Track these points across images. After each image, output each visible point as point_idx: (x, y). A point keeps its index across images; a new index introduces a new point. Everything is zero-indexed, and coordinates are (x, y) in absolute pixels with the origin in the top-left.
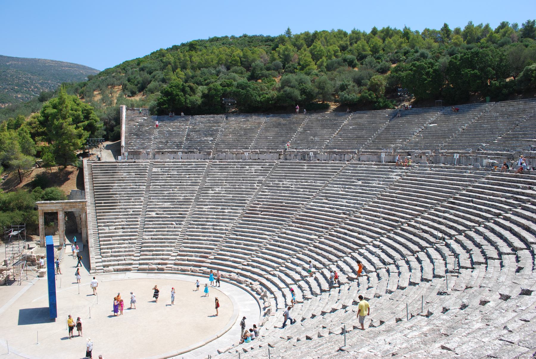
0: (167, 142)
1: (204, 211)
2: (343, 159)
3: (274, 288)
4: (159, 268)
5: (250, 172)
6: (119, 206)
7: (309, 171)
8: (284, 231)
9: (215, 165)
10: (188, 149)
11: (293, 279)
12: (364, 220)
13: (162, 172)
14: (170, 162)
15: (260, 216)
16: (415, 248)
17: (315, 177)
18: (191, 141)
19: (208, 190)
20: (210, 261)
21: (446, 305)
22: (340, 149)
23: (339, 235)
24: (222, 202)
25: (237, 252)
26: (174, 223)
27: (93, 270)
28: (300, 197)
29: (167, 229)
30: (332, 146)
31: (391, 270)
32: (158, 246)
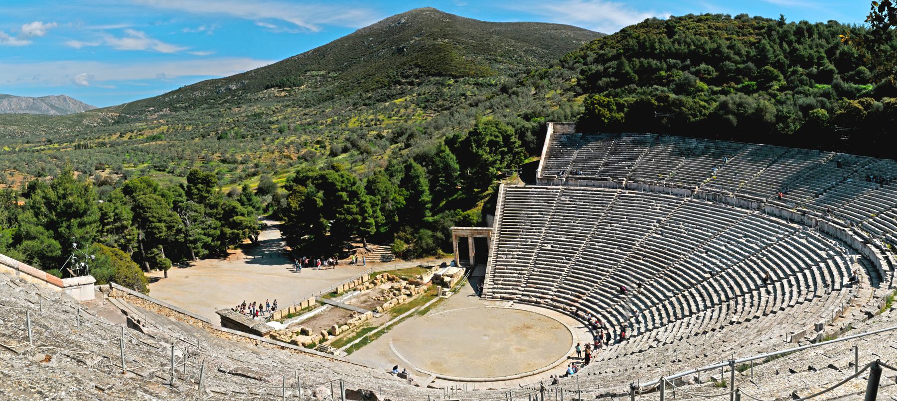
1: (596, 249)
6: (521, 235)
9: (623, 196)
24: (615, 241)
26: (564, 258)
29: (555, 264)
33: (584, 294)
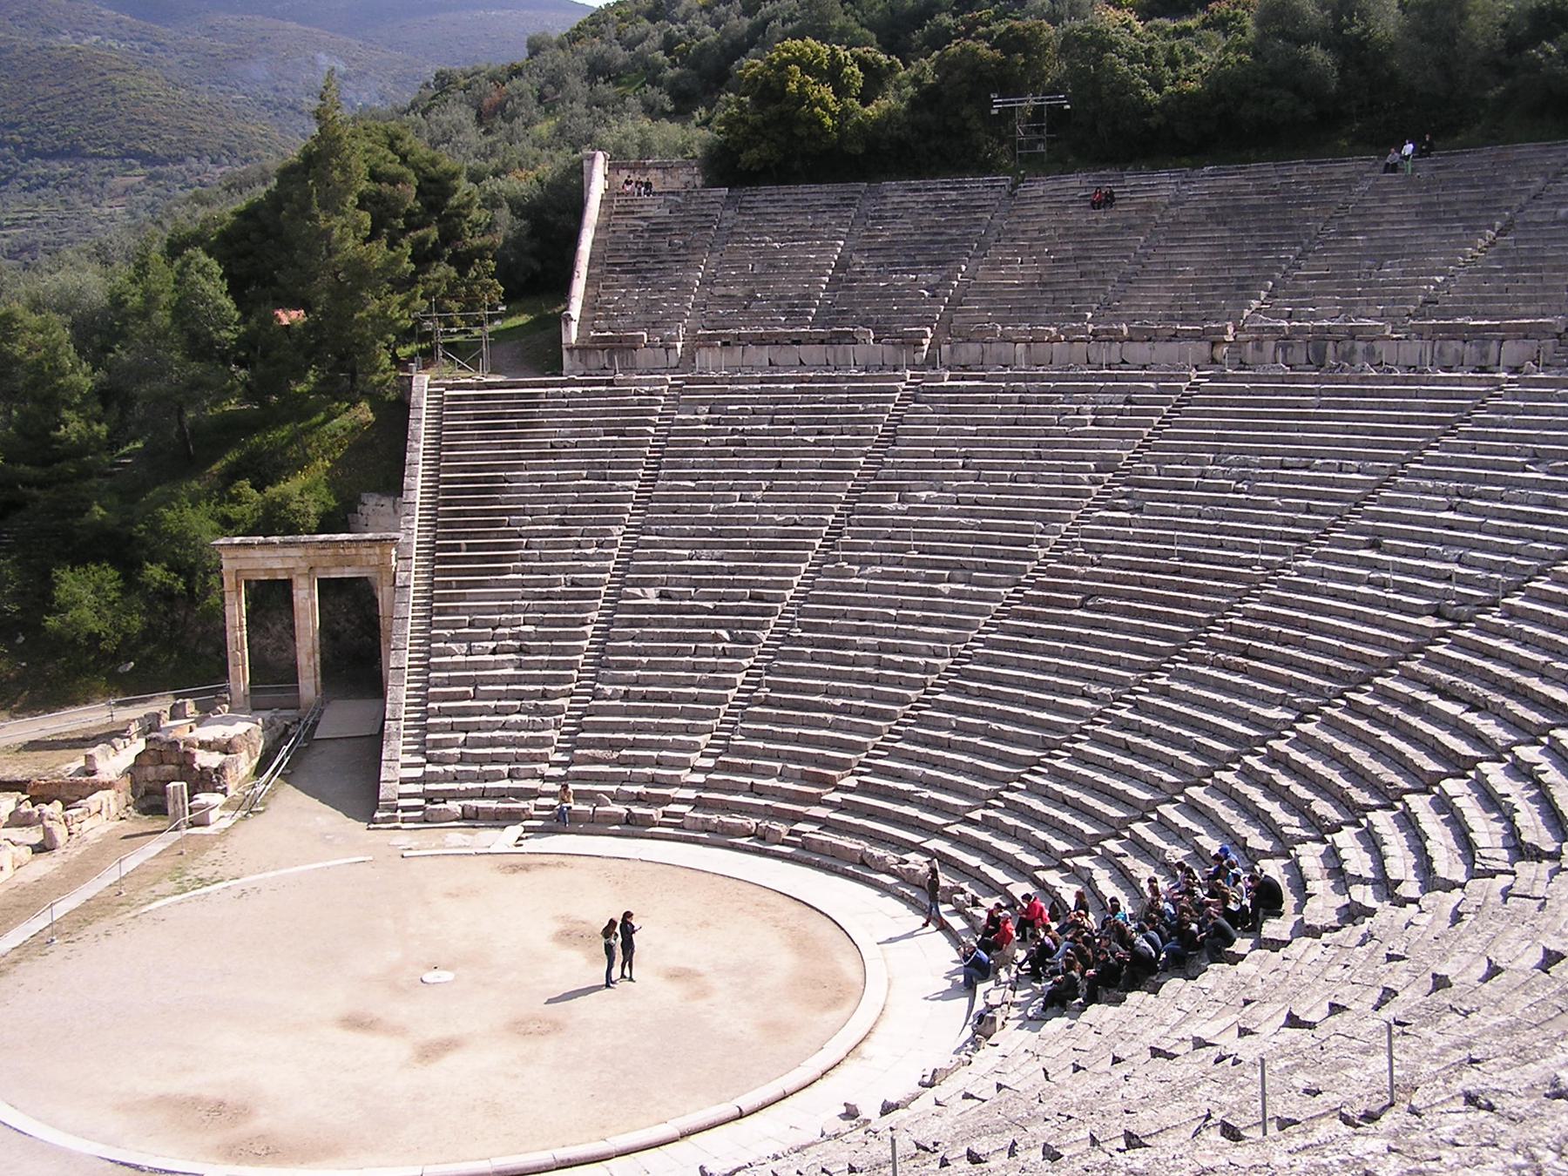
0: (751, 297)
2: (1492, 359)
5: (1074, 423)
7: (1328, 417)
9: (932, 390)
10: (834, 323)
14: (752, 381)
17: (1348, 443)
18: (851, 288)
20: (836, 797)
22: (1485, 316)
25: (954, 767)
27: (387, 808)
28: (1263, 535)
30: (1455, 300)
33: (842, 765)
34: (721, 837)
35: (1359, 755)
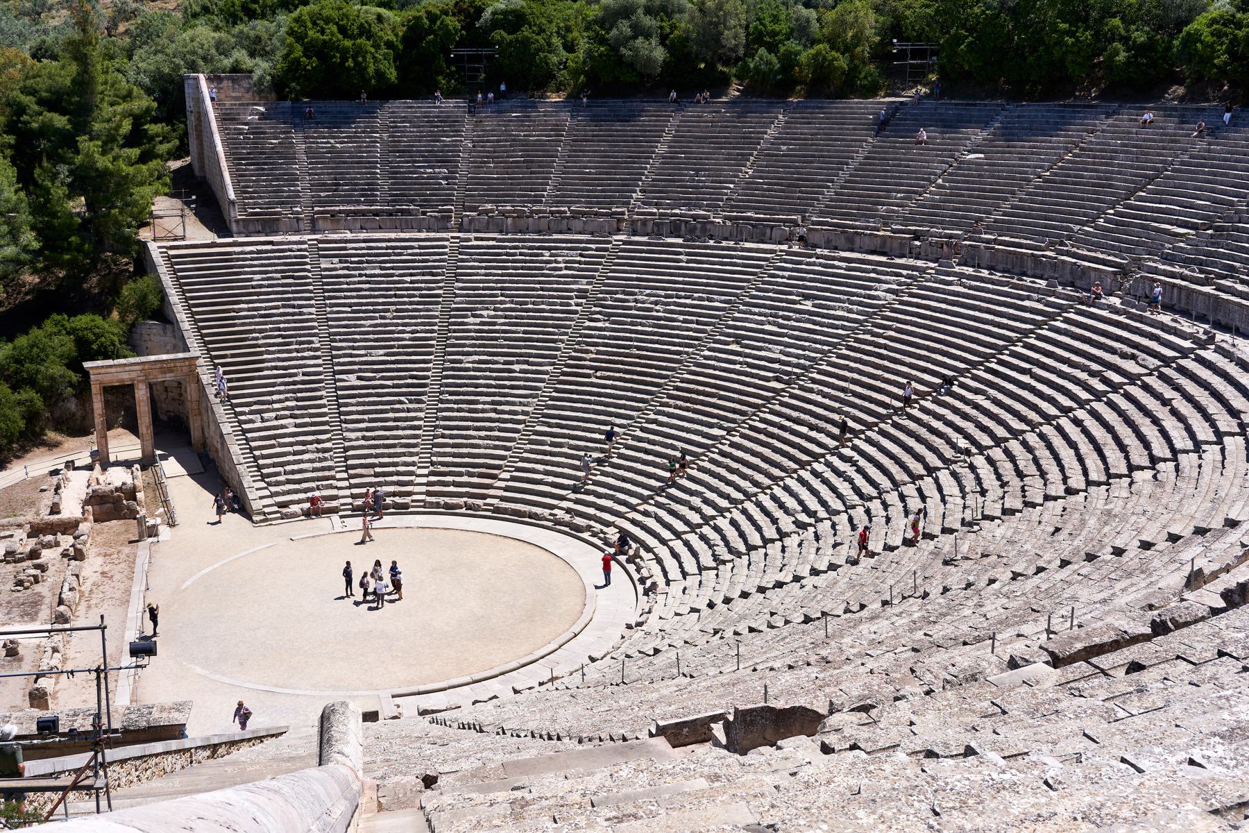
3: (652, 542)
4: (397, 503)
8: (652, 416)
11: (687, 522)
12: (819, 398)
13: (343, 268)
15: (594, 380)
16: (917, 468)
19: (465, 317)
20: (503, 484)
21: (948, 583)
23: (771, 429)
26: (402, 398)
27: (259, 514)
31: (873, 512)
32: (382, 455)
34: (450, 509)
35: (767, 452)
